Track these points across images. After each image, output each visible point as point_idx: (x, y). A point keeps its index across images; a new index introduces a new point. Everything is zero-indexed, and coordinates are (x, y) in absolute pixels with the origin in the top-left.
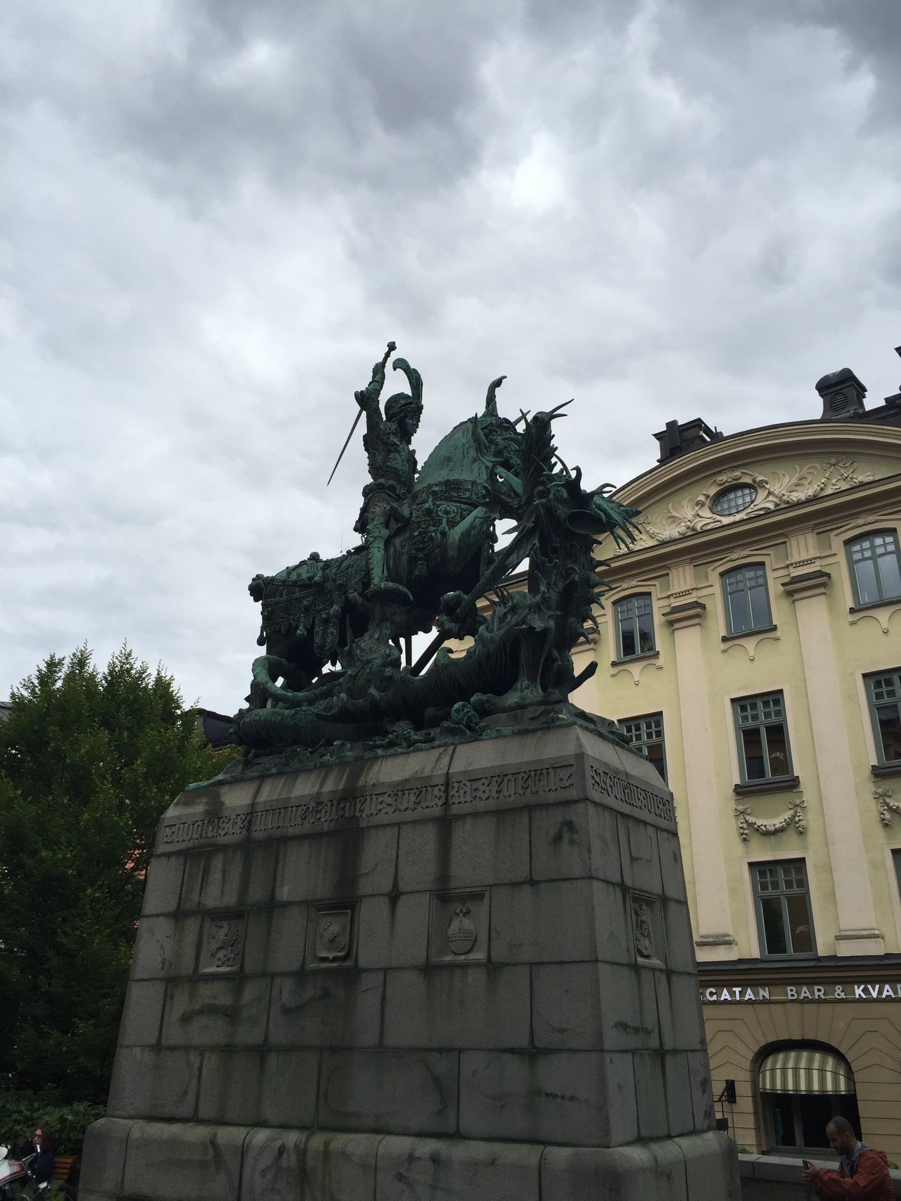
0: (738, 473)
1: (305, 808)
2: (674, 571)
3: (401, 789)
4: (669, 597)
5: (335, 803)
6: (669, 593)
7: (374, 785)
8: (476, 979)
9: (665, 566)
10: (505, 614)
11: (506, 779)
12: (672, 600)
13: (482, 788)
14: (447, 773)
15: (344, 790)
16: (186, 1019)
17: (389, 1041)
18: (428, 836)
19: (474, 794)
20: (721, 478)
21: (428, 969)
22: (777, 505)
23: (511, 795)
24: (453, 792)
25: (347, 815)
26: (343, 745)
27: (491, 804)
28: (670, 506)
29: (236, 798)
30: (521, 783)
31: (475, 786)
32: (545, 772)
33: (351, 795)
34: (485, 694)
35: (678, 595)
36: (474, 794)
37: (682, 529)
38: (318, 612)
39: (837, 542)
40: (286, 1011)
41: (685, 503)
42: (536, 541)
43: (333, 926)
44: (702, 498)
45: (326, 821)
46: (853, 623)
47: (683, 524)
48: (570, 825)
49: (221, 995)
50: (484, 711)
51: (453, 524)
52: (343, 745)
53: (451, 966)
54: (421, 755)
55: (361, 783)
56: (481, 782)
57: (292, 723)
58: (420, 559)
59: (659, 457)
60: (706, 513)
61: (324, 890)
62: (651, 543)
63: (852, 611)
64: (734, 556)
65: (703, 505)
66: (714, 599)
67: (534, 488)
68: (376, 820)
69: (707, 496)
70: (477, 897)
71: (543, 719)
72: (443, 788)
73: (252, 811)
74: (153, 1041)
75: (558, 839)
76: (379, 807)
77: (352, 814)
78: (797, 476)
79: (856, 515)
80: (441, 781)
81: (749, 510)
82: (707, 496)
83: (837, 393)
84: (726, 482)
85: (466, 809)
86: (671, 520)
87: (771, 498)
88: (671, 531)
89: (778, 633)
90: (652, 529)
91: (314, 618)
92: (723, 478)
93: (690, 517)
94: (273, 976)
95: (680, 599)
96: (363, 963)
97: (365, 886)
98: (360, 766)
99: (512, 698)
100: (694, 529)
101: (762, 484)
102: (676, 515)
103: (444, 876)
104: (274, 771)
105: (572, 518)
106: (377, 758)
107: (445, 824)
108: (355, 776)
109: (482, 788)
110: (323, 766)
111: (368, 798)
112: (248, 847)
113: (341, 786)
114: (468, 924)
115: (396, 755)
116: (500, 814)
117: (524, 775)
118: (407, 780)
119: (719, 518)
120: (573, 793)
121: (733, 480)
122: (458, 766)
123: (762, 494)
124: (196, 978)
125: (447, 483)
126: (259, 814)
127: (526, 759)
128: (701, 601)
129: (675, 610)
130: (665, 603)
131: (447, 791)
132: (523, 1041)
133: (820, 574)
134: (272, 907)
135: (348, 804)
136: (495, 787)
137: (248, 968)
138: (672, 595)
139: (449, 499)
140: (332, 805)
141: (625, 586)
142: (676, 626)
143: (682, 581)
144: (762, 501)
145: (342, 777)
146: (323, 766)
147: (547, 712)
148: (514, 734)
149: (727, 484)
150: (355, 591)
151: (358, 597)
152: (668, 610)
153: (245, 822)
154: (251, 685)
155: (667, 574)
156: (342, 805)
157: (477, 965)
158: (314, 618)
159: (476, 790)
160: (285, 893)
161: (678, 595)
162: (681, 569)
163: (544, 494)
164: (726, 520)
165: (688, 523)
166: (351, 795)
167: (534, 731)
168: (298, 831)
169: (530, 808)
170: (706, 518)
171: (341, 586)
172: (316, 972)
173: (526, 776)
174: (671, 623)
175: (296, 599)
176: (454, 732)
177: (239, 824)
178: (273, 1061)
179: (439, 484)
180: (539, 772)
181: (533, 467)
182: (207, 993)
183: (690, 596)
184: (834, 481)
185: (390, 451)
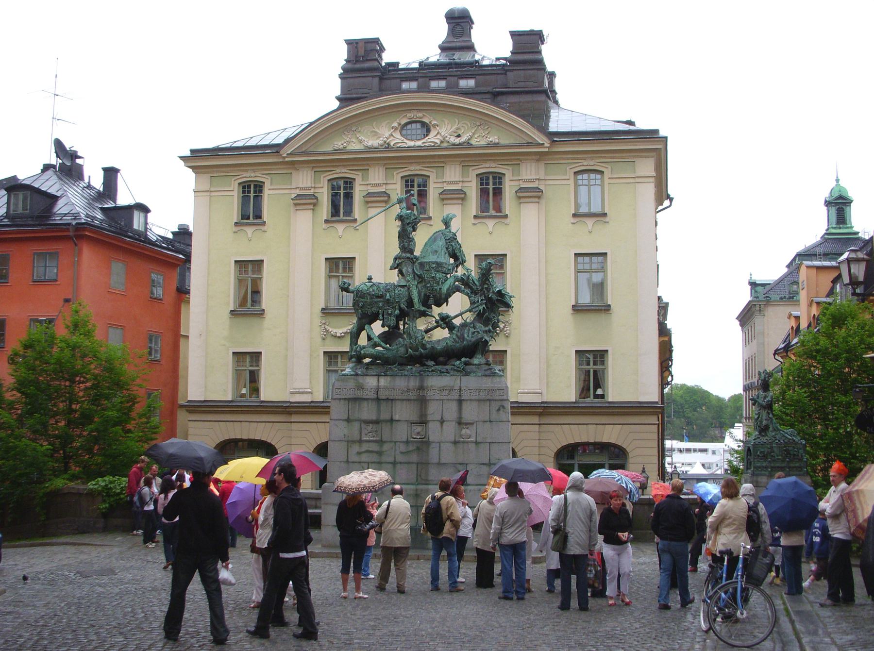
0: (420, 115)
3: (442, 389)
8: (472, 447)
12: (369, 187)
16: (359, 453)
17: (443, 461)
18: (454, 406)
21: (455, 443)
22: (442, 142)
23: (483, 396)
27: (477, 398)
29: (371, 382)
33: (421, 388)
37: (381, 142)
39: (473, 174)
40: (402, 453)
41: (384, 124)
43: (419, 429)
44: (395, 124)
45: (412, 395)
46: (474, 225)
48: (503, 407)
49: (374, 447)
50: (466, 364)
53: (463, 442)
55: (425, 385)
59: (346, 57)
60: (397, 135)
61: (414, 417)
63: (475, 217)
64: (412, 168)
65: (396, 129)
66: (397, 190)
68: (432, 398)
70: (472, 424)
71: (489, 372)
73: (378, 389)
74: (345, 460)
75: (499, 410)
78: (456, 126)
79: (485, 161)
82: (399, 124)
83: (458, 24)
85: (467, 398)
87: (438, 136)
89: (431, 222)
90: (362, 137)
93: (387, 135)
94: (395, 442)
96: (431, 439)
97: (429, 418)
99: (476, 361)
100: (389, 144)
101: (435, 126)
103: (460, 418)
105: (497, 300)
107: (460, 401)
108: (422, 381)
110: (405, 375)
112: (378, 400)
114: (468, 431)
116: (479, 400)
119: (405, 141)
120: (505, 397)
123: (433, 133)
124: (360, 441)
125: (437, 263)
129: (370, 194)
132: (487, 461)
133: (461, 191)
134: (392, 420)
137: (384, 439)
139: (439, 271)
141: (338, 171)
144: (433, 138)
146: (405, 375)
147: (491, 369)
157: (472, 442)
160: (397, 417)
162: (377, 169)
163: (488, 289)
164: (411, 143)
166: (421, 388)
168: (400, 397)
169: (490, 400)
170: (397, 139)
172: (412, 442)
176: (458, 371)
178: (398, 466)
179: (434, 263)
182: (365, 447)
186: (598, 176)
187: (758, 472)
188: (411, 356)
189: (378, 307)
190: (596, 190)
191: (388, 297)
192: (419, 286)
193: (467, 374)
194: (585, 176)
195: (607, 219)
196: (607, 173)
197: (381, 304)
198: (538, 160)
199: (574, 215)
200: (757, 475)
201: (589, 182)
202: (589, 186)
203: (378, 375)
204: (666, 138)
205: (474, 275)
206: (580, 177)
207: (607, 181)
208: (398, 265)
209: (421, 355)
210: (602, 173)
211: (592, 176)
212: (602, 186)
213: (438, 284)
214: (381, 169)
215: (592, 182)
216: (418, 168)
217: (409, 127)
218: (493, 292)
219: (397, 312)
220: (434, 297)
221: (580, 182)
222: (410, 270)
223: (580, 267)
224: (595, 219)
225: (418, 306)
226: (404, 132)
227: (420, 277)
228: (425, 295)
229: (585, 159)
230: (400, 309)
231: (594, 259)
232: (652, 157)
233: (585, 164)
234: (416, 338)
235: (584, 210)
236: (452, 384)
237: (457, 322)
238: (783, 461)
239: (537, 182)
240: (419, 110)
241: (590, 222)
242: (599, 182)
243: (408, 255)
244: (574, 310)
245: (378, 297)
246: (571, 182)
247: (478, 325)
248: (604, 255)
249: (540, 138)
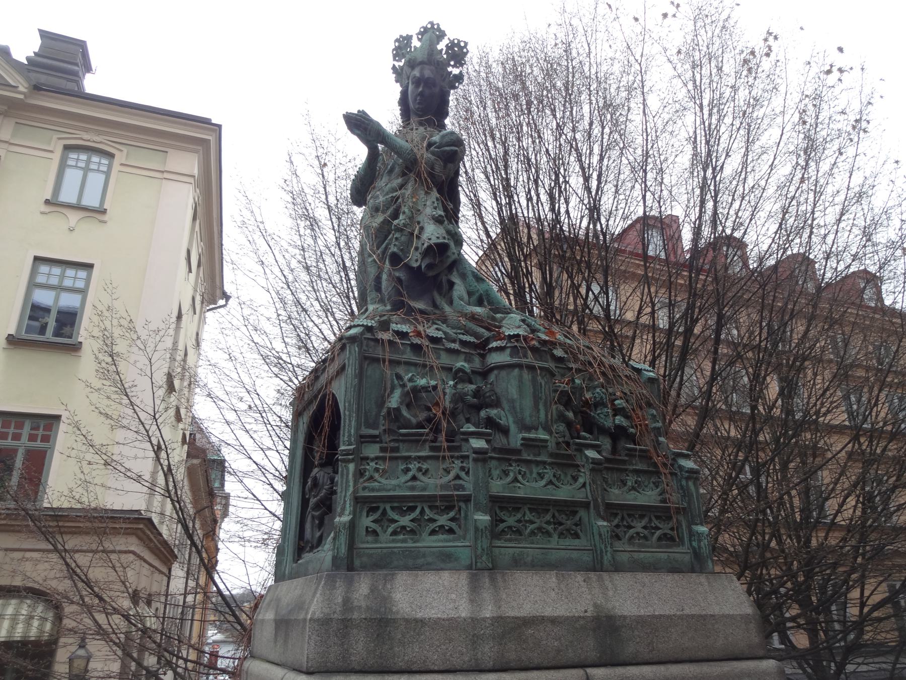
186: (105, 161)
187: (386, 541)
190: (96, 180)
194: (83, 157)
195: (105, 218)
196: (119, 158)
199: (47, 202)
200: (384, 564)
202: (86, 170)
204: (220, 126)
206: (73, 156)
210: (111, 156)
211: (95, 159)
212: (108, 174)
221: (70, 162)
223: (41, 279)
224: (82, 214)
229: (87, 130)
231: (70, 272)
232: (196, 152)
235: (68, 195)
238: (565, 463)
241: (74, 217)
242: (105, 169)
246: (57, 156)
248: (89, 267)
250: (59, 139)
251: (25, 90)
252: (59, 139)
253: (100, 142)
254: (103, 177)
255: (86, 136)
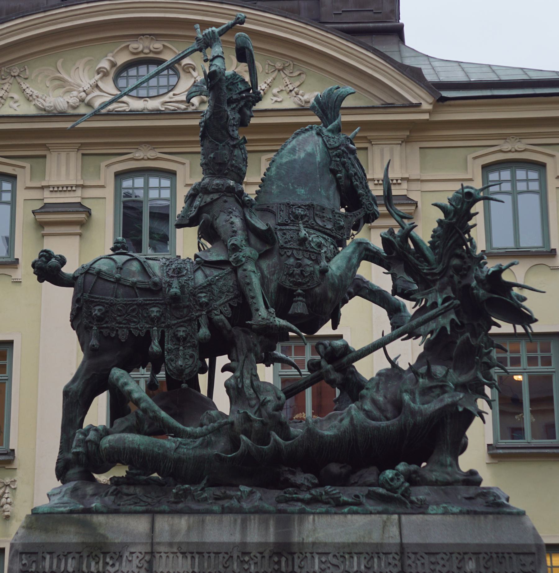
0: (158, 45)
1: (227, 557)
2: (55, 155)
3: (348, 551)
4: (43, 188)
5: (266, 554)
6: (44, 183)
7: (314, 544)
9: (44, 145)
10: (431, 388)
11: (466, 557)
12: (47, 193)
13: (441, 562)
14: (401, 544)
15: (277, 544)
19: (432, 567)
20: (135, 45)
24: (410, 562)
25: (283, 569)
26: (251, 493)
28: (59, 63)
30: (482, 562)
31: (433, 559)
32: (507, 556)
34: (410, 463)
35: (56, 189)
36: (432, 567)
37: (73, 101)
38: (168, 327)
41: (81, 64)
42: (453, 316)
44: (105, 64)
47: (75, 93)
51: (329, 260)
52: (251, 493)
54: (359, 520)
56: (439, 556)
57: (176, 456)
58: (299, 295)
62: (31, 110)
64: (139, 154)
65: (106, 74)
67: (450, 258)
69: (113, 64)
72: (397, 557)
76: (323, 566)
77: (290, 569)
80: (397, 549)
81: (166, 98)
82: (113, 64)
84: (142, 52)
86: (57, 82)
88: (58, 100)
91: (163, 333)
92: (137, 46)
93: (86, 86)
95: (58, 195)
98: (284, 519)
102: (66, 77)
104: (165, 507)
105: (490, 301)
106: (302, 512)
109: (441, 562)
111: (308, 555)
113: (271, 539)
115: (327, 513)
117: (485, 556)
118: (354, 544)
121: (151, 51)
122: (412, 537)
125: (310, 207)
126: (164, 556)
127: (486, 541)
128: (86, 203)
129: (47, 208)
130: (36, 194)
131: (401, 560)
135: (283, 560)
136: (455, 563)
138: (48, 187)
140: (263, 557)
142: (47, 230)
143: (63, 169)
145: (267, 528)
148: (461, 513)
149: (142, 56)
150: (221, 313)
151: (226, 322)
152: (37, 206)
153: (143, 561)
154: (63, 392)
155: (44, 157)
156: (276, 559)
158: (163, 333)
159: (433, 563)
161: (56, 189)
162: (63, 155)
163: (463, 271)
165: (83, 94)
166: (284, 550)
167: (486, 514)
171: (207, 304)
173: (487, 557)
174: (41, 225)
175: (139, 305)
177: (136, 562)
180: (500, 555)
181: (453, 239)
183: (72, 194)
184: (275, 91)
185: (234, 146)
186: (533, 175)
188: (248, 458)
189: (152, 321)
190: (529, 204)
191: (175, 290)
192: (265, 264)
193: (421, 508)
194: (506, 175)
197: (155, 311)
198: (406, 141)
201: (514, 186)
202: (514, 193)
203: (152, 513)
205: (425, 231)
206: (493, 176)
207: (552, 183)
208: (201, 210)
209: (278, 458)
211: (521, 174)
212: (543, 193)
213: (317, 261)
214: (73, 155)
215: (521, 186)
216: (152, 154)
217: (133, 72)
218: (477, 278)
219: (204, 332)
220: (307, 294)
222: (238, 222)
225: (263, 313)
226: (122, 83)
227: (266, 237)
228: (281, 289)
229: (504, 137)
230: (212, 325)
233: (507, 147)
234: (263, 404)
236: (376, 538)
237: (368, 368)
239: (405, 185)
240: (157, 37)
242: (535, 186)
243: (232, 183)
244: (493, 456)
245: (146, 291)
247: (439, 370)
249: (411, 93)
250: (475, 158)
251: (430, 107)
252: (475, 158)
253: (525, 150)
254: (536, 197)
255: (507, 147)
